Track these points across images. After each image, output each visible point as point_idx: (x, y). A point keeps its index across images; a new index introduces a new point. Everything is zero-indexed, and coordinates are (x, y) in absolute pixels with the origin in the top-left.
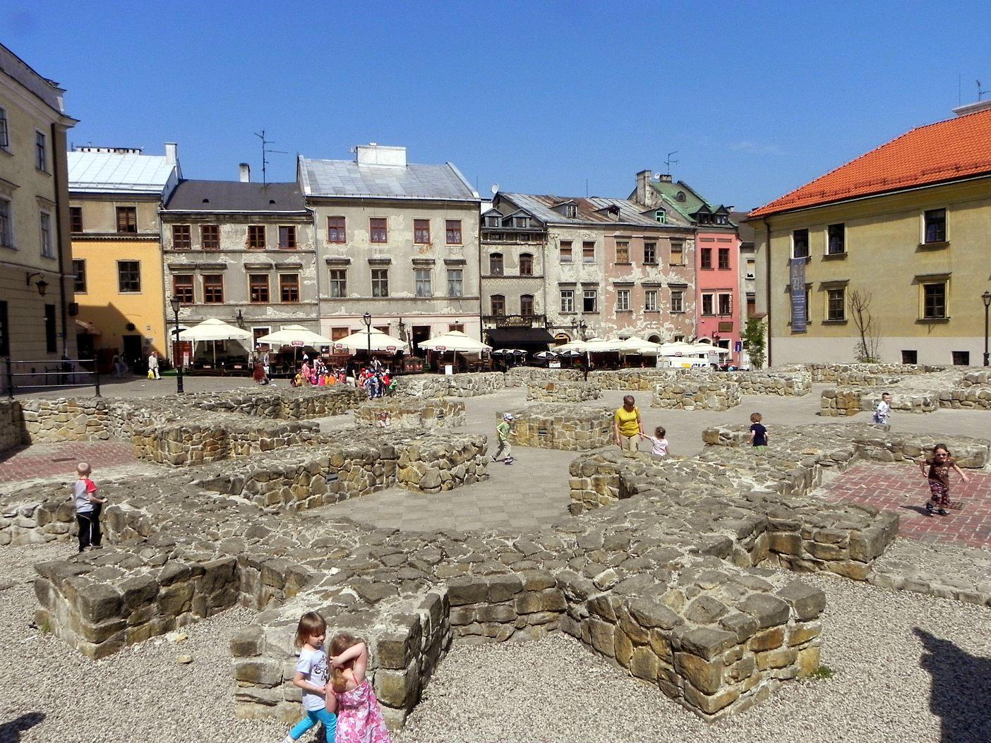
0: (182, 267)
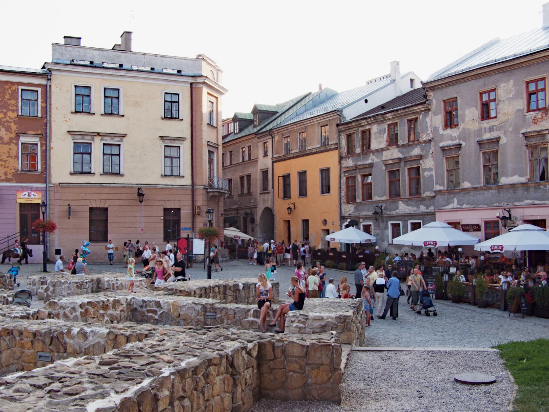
0: (349, 170)
